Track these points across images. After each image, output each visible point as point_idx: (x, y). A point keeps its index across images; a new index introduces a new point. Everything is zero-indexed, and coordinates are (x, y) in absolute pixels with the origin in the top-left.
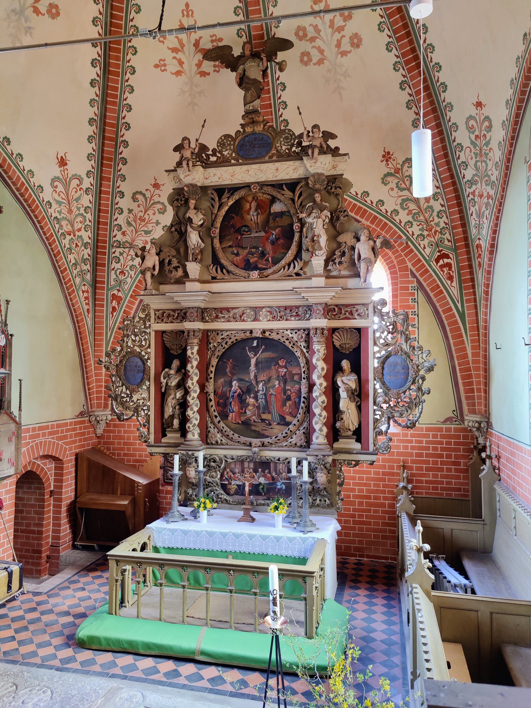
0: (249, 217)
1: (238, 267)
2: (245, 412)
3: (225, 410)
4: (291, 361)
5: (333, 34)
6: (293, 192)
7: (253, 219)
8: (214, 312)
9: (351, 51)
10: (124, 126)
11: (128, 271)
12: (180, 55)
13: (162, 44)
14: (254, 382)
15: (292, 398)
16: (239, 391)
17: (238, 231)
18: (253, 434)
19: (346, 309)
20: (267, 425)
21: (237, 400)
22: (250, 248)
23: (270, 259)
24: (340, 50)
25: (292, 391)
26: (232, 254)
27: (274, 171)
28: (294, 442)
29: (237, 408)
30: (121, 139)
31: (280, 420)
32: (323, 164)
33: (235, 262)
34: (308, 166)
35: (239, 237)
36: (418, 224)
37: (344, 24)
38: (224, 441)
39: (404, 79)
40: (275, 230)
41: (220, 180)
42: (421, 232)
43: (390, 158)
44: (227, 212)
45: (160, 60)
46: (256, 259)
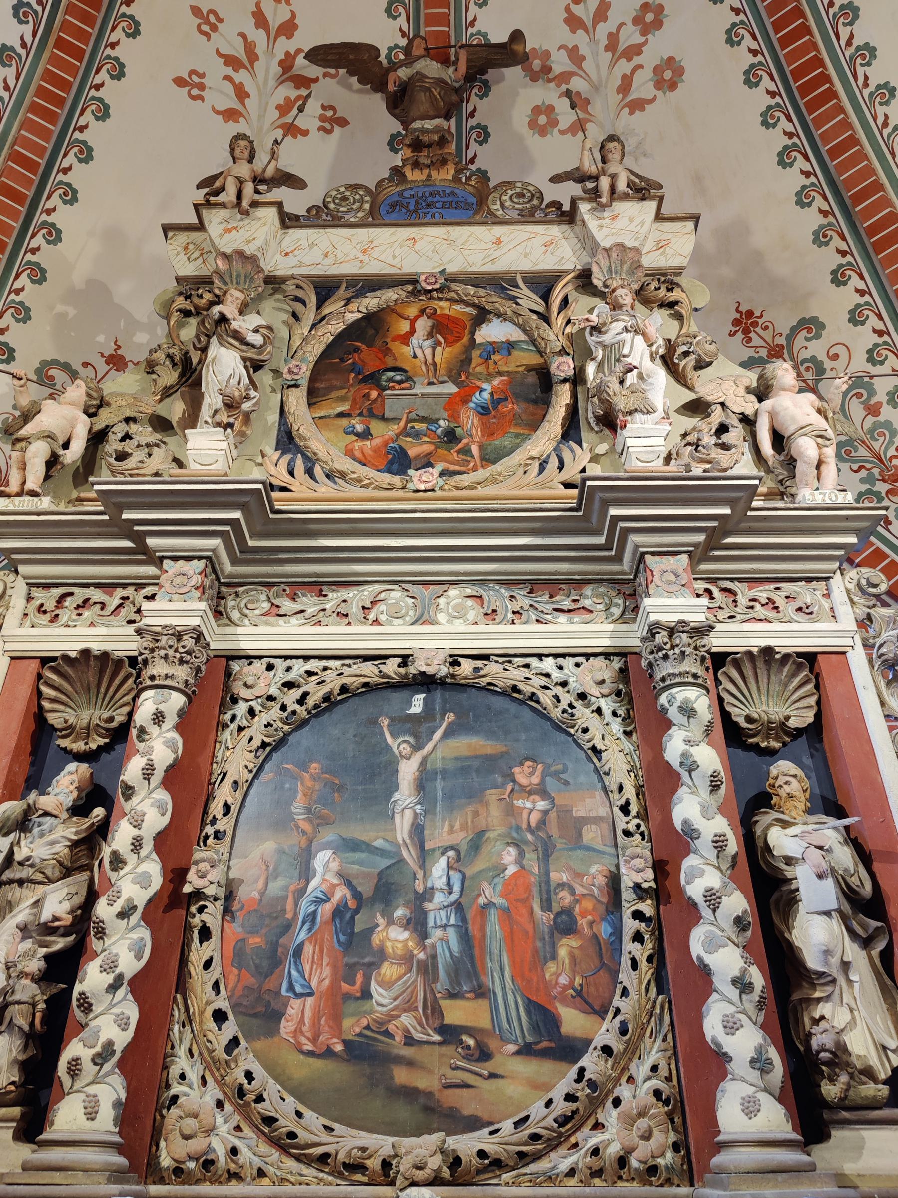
0: (407, 351)
1: (364, 465)
2: (366, 994)
3: (270, 984)
4: (564, 771)
5: (613, 64)
6: (546, 297)
7: (419, 353)
9: (654, 99)
10: (61, 191)
12: (241, 77)
13: (205, 38)
14: (409, 856)
15: (583, 923)
16: (341, 893)
17: (372, 379)
18: (403, 1112)
19: (752, 593)
20: (468, 1058)
21: (328, 936)
22: (409, 421)
23: (475, 449)
24: (628, 100)
25: (579, 890)
26: (347, 433)
27: (490, 245)
28: (613, 1150)
29: (327, 972)
30: (44, 217)
31: (535, 1028)
32: (637, 221)
33: (358, 454)
34: (592, 224)
35: (374, 394)
36: (855, 466)
37: (643, 39)
38: (246, 1155)
39: (789, 142)
40: (488, 381)
41: (328, 261)
42: (867, 486)
43: (755, 325)
44: (340, 338)
45: (192, 72)
46: (427, 448)
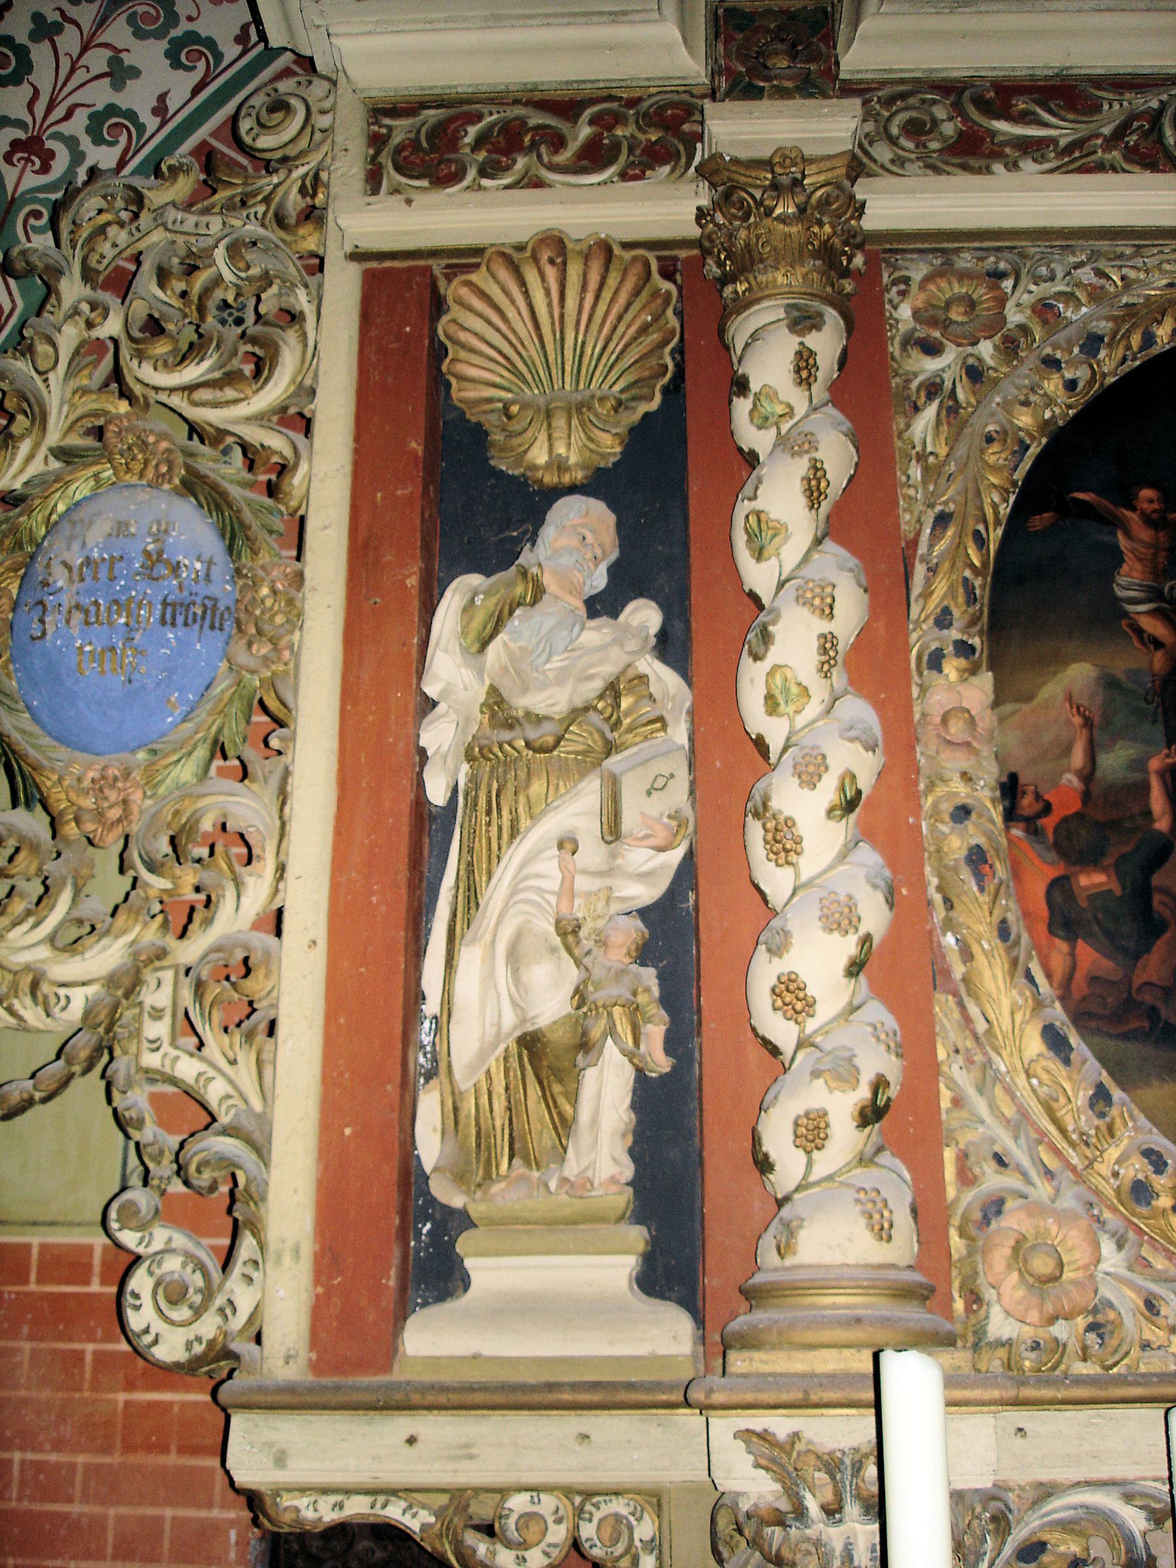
8: (940, 112)
11: (71, 142)
